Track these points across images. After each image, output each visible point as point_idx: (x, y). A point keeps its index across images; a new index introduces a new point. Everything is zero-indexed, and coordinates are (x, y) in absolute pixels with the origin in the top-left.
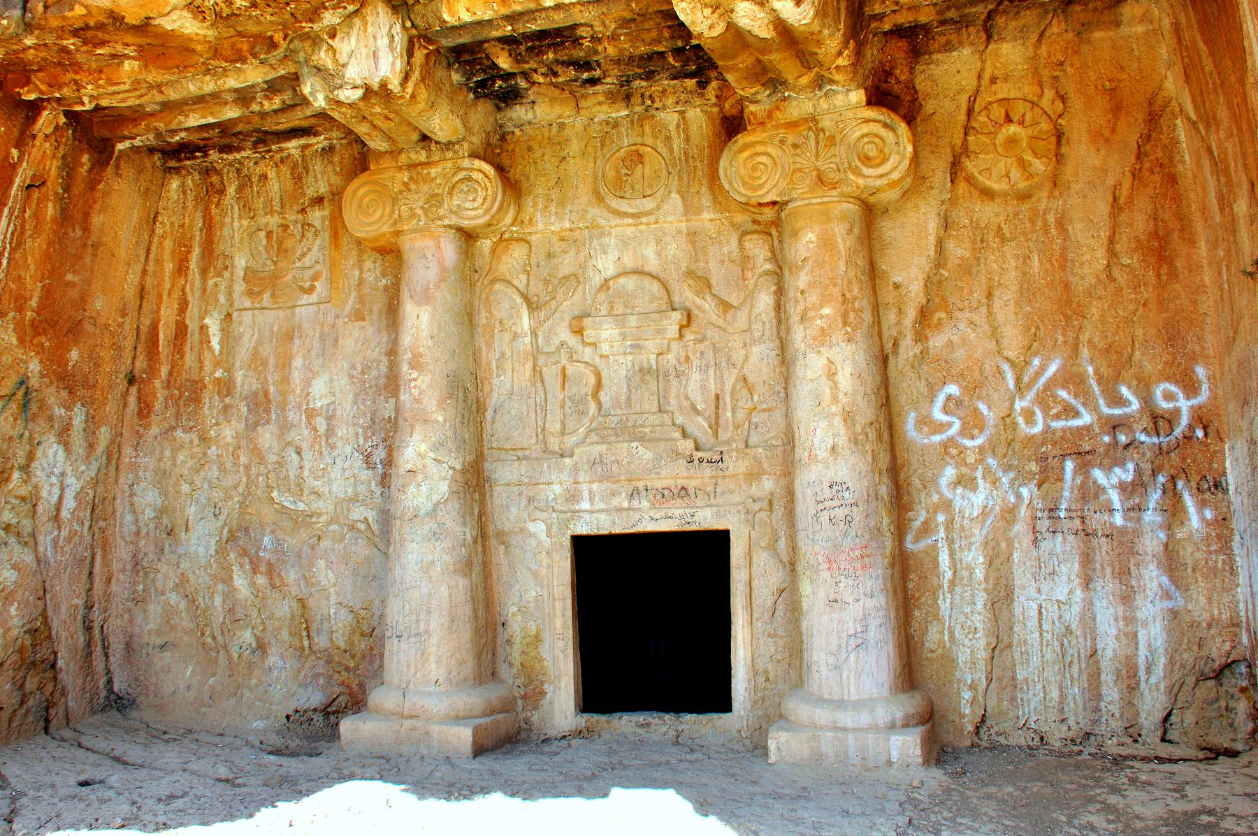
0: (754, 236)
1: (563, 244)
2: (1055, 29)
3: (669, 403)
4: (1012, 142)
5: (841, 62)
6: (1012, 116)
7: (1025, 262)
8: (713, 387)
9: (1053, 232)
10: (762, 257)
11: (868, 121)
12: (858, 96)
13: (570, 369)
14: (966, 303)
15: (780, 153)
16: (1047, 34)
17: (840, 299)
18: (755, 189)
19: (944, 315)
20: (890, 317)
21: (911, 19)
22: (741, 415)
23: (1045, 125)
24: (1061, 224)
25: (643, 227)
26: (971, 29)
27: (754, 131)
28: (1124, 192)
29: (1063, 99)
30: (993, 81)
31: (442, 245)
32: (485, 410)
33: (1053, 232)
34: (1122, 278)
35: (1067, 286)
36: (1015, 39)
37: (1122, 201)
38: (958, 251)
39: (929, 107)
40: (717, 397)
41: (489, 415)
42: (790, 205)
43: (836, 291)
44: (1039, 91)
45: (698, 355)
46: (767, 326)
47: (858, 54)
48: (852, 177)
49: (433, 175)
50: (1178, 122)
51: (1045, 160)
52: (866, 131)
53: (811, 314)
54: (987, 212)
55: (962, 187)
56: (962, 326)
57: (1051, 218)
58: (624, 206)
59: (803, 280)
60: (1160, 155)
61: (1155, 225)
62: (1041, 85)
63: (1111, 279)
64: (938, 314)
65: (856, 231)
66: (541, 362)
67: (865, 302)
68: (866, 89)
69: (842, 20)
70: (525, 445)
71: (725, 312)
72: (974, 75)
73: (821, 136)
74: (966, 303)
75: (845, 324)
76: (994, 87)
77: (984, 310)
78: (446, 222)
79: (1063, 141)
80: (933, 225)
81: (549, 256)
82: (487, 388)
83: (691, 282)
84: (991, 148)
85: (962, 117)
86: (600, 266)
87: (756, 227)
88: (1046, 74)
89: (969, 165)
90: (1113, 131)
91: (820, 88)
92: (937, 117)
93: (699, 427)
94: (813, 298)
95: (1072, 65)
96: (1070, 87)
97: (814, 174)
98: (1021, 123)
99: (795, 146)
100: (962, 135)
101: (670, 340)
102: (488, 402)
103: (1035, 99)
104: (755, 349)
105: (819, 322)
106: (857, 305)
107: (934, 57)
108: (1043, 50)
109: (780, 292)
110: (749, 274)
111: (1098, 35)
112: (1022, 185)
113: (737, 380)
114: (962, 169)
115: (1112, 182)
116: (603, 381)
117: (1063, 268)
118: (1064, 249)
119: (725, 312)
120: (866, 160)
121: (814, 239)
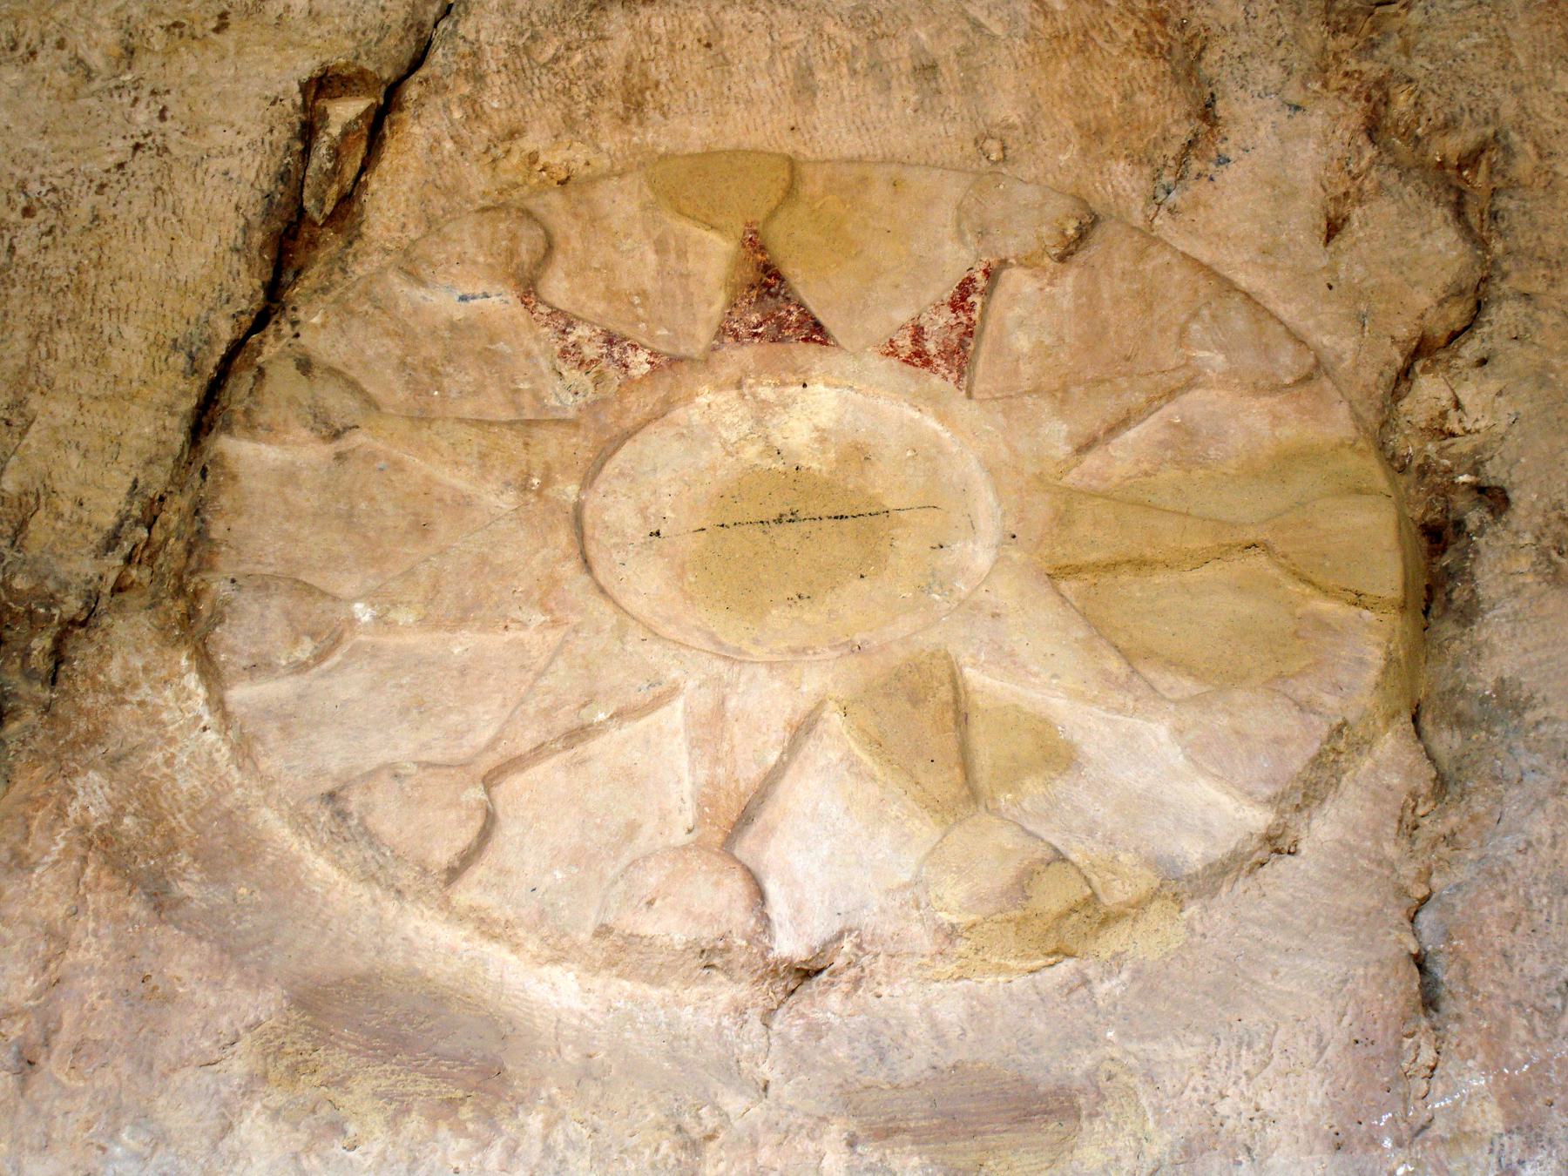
62: (1180, 51)
98: (947, 347)
100: (154, 425)
112: (936, 1007)
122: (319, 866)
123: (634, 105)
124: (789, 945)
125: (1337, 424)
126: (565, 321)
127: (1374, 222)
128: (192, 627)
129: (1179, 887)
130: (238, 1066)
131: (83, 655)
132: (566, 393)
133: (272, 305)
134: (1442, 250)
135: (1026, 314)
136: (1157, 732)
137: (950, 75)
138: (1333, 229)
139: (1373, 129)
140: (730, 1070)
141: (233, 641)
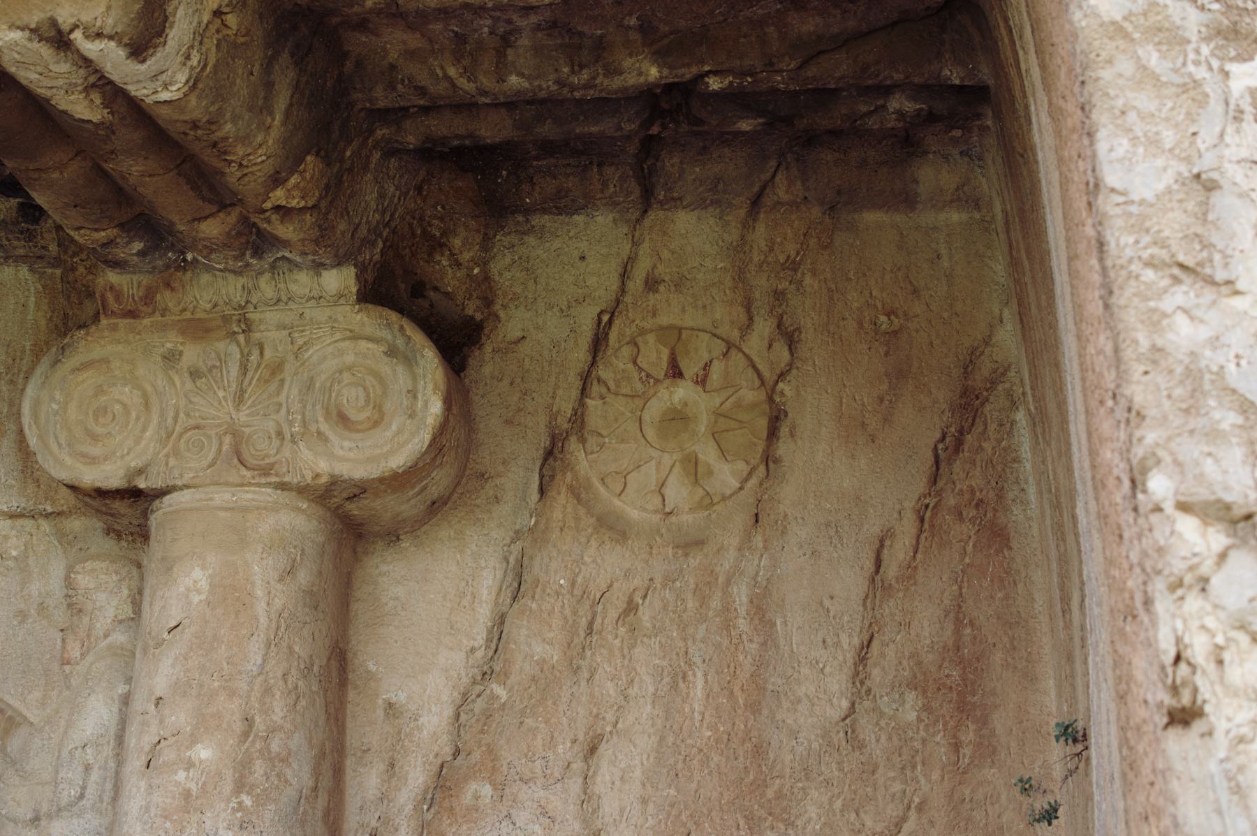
0: (98, 565)
2: (781, 191)
4: (678, 419)
5: (278, 196)
6: (683, 364)
7: (674, 686)
9: (742, 624)
10: (110, 613)
11: (355, 337)
12: (341, 280)
14: (538, 765)
15: (161, 382)
16: (768, 200)
17: (239, 727)
18: (93, 461)
19: (487, 790)
20: (365, 782)
21: (461, 131)
23: (750, 394)
24: (760, 611)
26: (608, 171)
27: (114, 328)
28: (898, 553)
29: (791, 338)
30: (652, 284)
33: (742, 624)
34: (877, 744)
35: (759, 751)
36: (701, 204)
37: (891, 570)
38: (535, 644)
39: (513, 322)
42: (167, 499)
43: (232, 710)
44: (743, 318)
46: (95, 776)
47: (334, 192)
48: (305, 453)
50: (1020, 416)
51: (741, 466)
52: (350, 359)
53: (168, 755)
54: (607, 566)
55: (561, 501)
56: (522, 817)
57: (741, 594)
59: (162, 675)
60: (977, 482)
61: (957, 632)
63: (851, 735)
64: (473, 786)
65: (303, 577)
67: (297, 741)
68: (361, 270)
69: (281, 104)
72: (612, 269)
73: (254, 358)
74: (538, 765)
75: (241, 786)
76: (652, 299)
77: (575, 785)
79: (784, 431)
80: (489, 583)
84: (633, 427)
85: (580, 355)
87: (109, 544)
88: (761, 284)
89: (582, 459)
90: (887, 420)
91: (258, 253)
92: (525, 348)
94: (180, 717)
95: (814, 273)
96: (806, 314)
97: (228, 439)
98: (702, 381)
99: (195, 374)
100: (575, 393)
103: (735, 334)
105: (181, 775)
106: (275, 746)
107: (537, 220)
108: (760, 233)
109: (126, 700)
110: (75, 652)
111: (872, 217)
112: (687, 518)
114: (568, 467)
115: (876, 530)
117: (754, 708)
118: (760, 664)
120: (343, 420)
121: (204, 584)
122: (602, 490)
123: (654, 315)
124: (667, 510)
125: (763, 396)
126: (641, 369)
127: (776, 345)
128: (583, 440)
129: (724, 498)
130: (590, 530)
131: (566, 446)
132: (639, 387)
133: (594, 363)
134: (786, 355)
135: (717, 369)
136: (726, 467)
137: (709, 308)
138: (770, 346)
139: (779, 326)
140: (658, 531)
141: (588, 445)
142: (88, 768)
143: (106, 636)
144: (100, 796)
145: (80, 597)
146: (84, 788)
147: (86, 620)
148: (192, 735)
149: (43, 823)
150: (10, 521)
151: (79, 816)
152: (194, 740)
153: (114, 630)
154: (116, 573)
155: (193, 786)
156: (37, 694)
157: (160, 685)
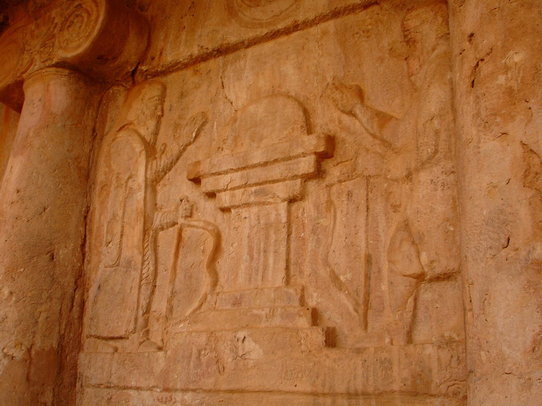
1: (196, 79)
3: (301, 272)
8: (363, 244)
13: (187, 233)
22: (403, 287)
25: (283, 39)
31: (52, 88)
32: (91, 286)
40: (369, 260)
41: (92, 292)
45: (344, 198)
49: (53, 15)
53: (486, 69)
58: (258, 14)
66: (157, 223)
70: (122, 333)
71: (382, 126)
78: (55, 61)
81: (182, 95)
82: (94, 259)
83: (337, 95)
86: (232, 97)
93: (338, 310)
101: (307, 178)
102: (93, 276)
104: (424, 176)
105: (501, 79)
113: (398, 230)
116: (223, 244)
119: (382, 126)
142: (437, 133)
143: (433, 50)
144: (449, 148)
145: (412, 34)
146: (437, 145)
147: (419, 45)
148: (503, 47)
149: (414, 176)
150: (364, 11)
151: (436, 165)
152: (506, 49)
153: (438, 44)
154: (432, 11)
155: (514, 85)
156: (397, 101)
157: (469, 26)
